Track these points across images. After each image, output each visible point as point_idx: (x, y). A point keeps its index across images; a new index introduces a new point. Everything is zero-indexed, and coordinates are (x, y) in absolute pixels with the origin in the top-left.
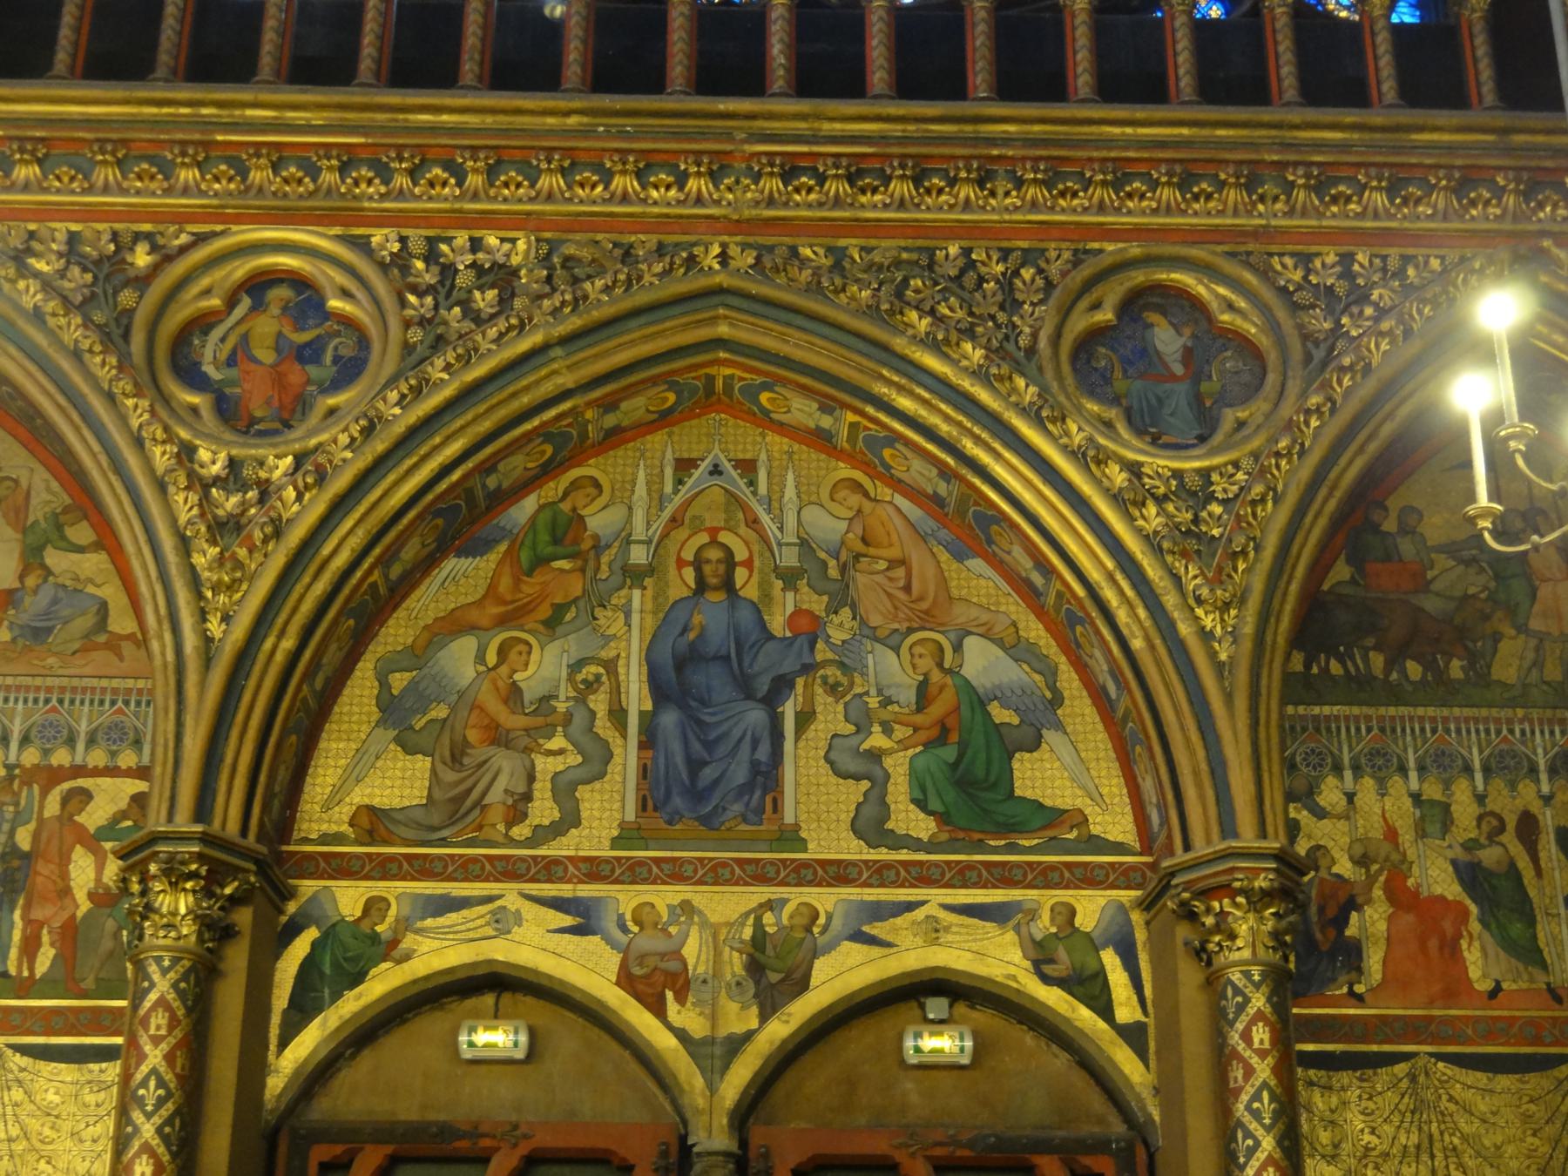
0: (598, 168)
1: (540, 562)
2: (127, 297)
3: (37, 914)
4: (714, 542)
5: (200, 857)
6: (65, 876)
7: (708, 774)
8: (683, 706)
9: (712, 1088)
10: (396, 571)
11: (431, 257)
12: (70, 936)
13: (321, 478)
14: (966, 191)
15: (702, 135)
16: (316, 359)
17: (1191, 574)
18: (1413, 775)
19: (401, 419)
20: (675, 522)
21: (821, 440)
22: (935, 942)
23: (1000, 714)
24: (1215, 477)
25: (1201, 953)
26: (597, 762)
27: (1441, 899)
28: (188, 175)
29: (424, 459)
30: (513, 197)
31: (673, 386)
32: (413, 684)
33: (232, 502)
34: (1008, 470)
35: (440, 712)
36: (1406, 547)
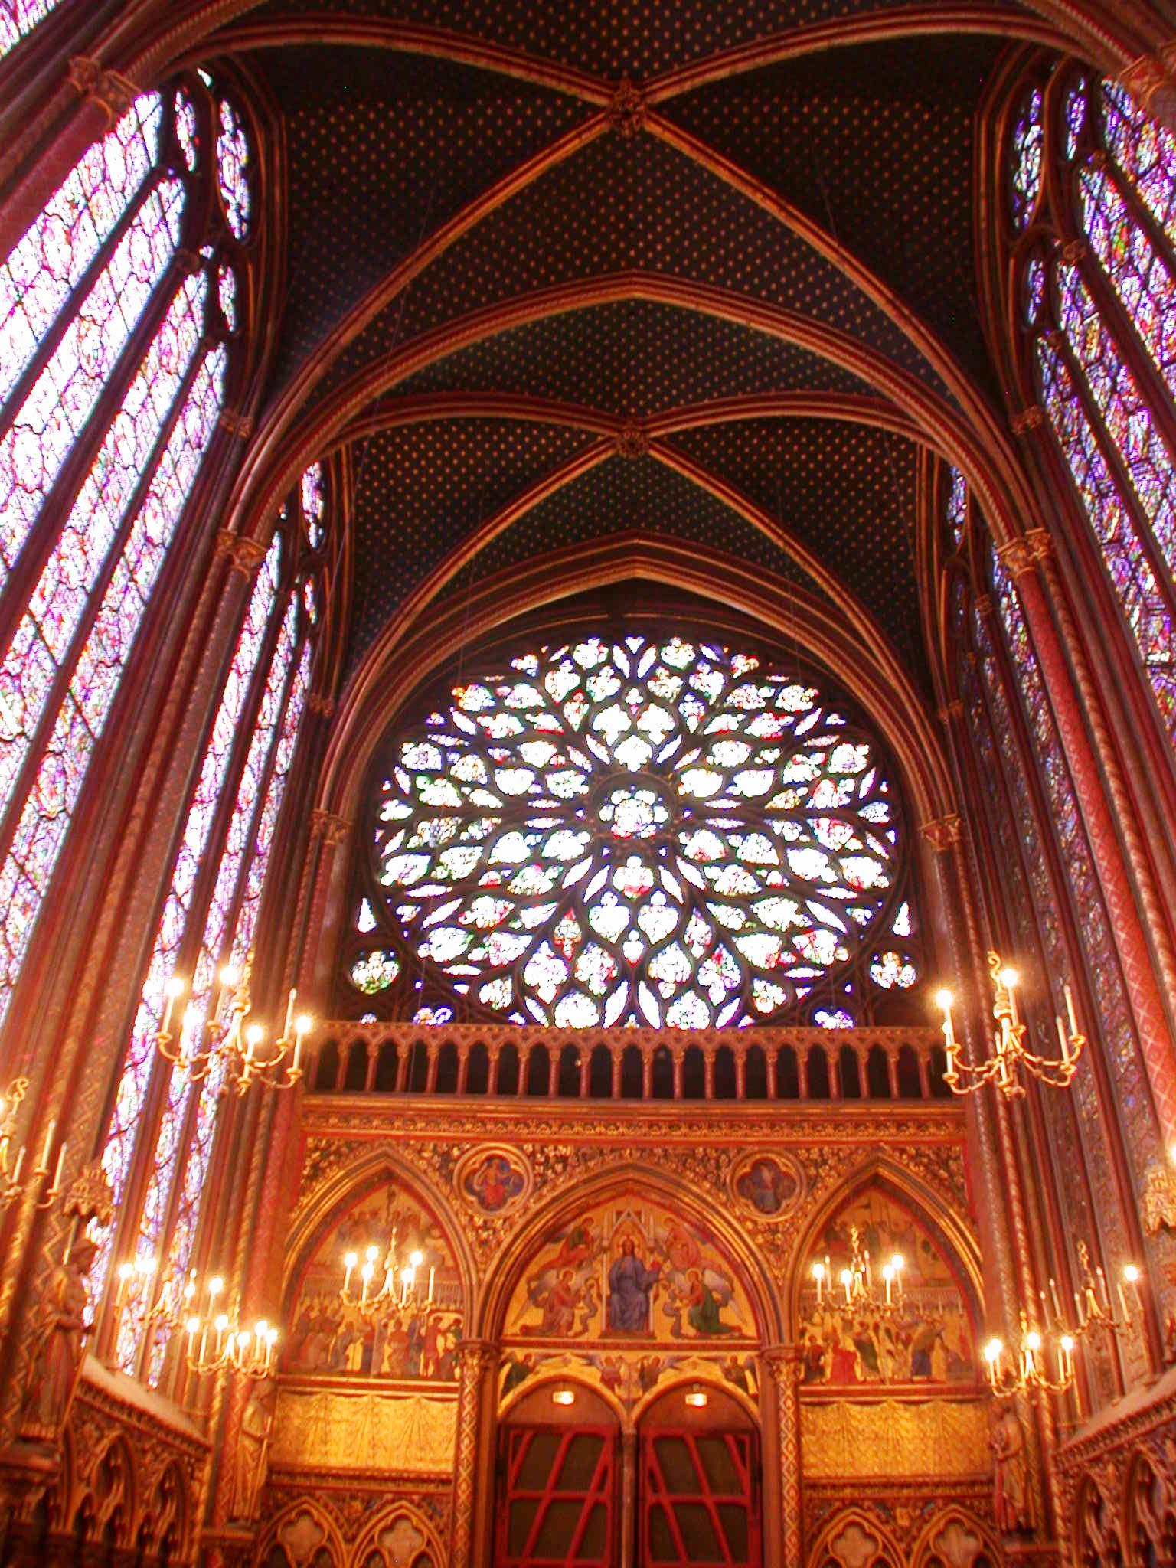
1: (575, 1246)
12: (438, 1363)
19: (534, 1207)
23: (716, 1295)
25: (772, 1374)
30: (566, 1132)
33: (485, 1235)
34: (716, 1221)
35: (546, 1295)
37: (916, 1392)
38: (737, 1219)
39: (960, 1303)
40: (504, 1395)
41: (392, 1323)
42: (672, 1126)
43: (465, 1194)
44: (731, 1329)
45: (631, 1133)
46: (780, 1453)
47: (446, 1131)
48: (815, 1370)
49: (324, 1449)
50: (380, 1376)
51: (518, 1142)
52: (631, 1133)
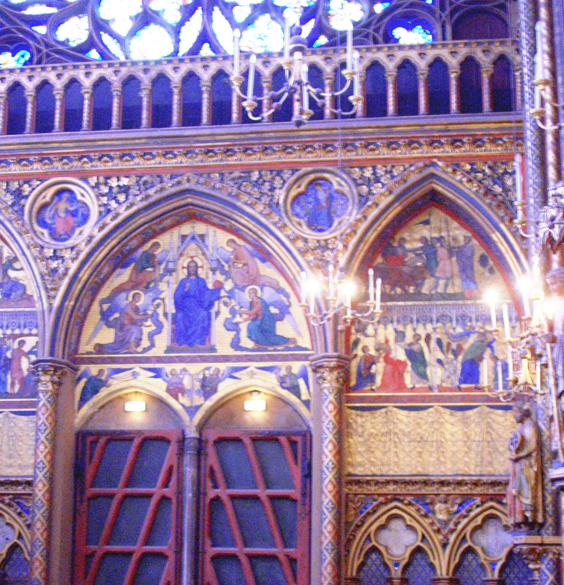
1: (144, 268)
2: (23, 202)
3: (14, 376)
6: (20, 365)
7: (190, 332)
10: (102, 277)
11: (106, 184)
13: (78, 254)
19: (99, 236)
21: (223, 228)
22: (252, 378)
23: (273, 310)
24: (329, 242)
26: (159, 327)
29: (106, 246)
32: (110, 307)
34: (271, 240)
35: (117, 315)
36: (400, 251)
37: (463, 399)
38: (288, 237)
42: (228, 152)
47: (16, 169)
48: (366, 377)
51: (84, 176)
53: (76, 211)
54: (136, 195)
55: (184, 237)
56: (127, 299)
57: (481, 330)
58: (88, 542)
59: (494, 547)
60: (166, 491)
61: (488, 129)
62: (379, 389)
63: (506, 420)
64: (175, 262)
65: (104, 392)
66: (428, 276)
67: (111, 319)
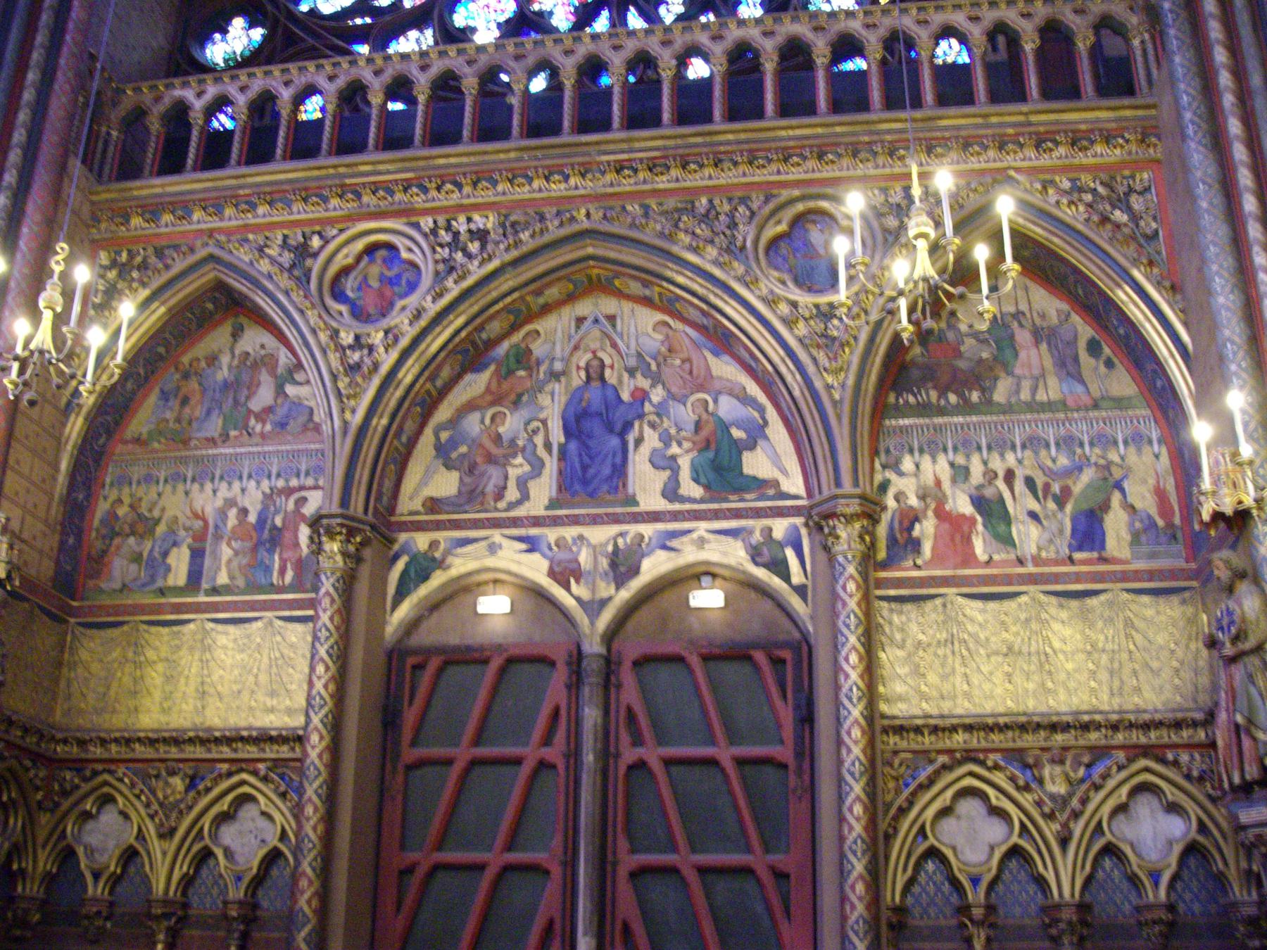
0: (526, 176)
1: (511, 372)
2: (309, 262)
3: (285, 556)
4: (595, 356)
5: (342, 525)
6: (296, 537)
7: (592, 471)
8: (578, 437)
9: (592, 624)
10: (439, 383)
11: (448, 228)
13: (396, 339)
14: (708, 171)
15: (576, 155)
16: (398, 284)
17: (821, 356)
18: (951, 453)
19: (433, 308)
20: (576, 348)
21: (647, 302)
23: (737, 433)
25: (827, 549)
26: (537, 467)
27: (963, 516)
28: (335, 202)
30: (485, 195)
31: (570, 280)
33: (355, 357)
34: (732, 309)
35: (463, 449)
37: (1078, 578)
39: (1155, 435)
40: (395, 606)
41: (233, 513)
43: (330, 302)
44: (760, 485)
45: (588, 186)
46: (837, 669)
47: (300, 212)
49: (131, 703)
50: (215, 591)
52: (588, 186)
53: (399, 276)
54: (497, 243)
55: (580, 321)
56: (482, 422)
57: (1102, 462)
58: (402, 847)
59: (1149, 842)
60: (546, 752)
61: (1098, 120)
62: (928, 564)
63: (1158, 613)
64: (567, 361)
65: (437, 579)
66: (1003, 375)
67: (454, 455)
